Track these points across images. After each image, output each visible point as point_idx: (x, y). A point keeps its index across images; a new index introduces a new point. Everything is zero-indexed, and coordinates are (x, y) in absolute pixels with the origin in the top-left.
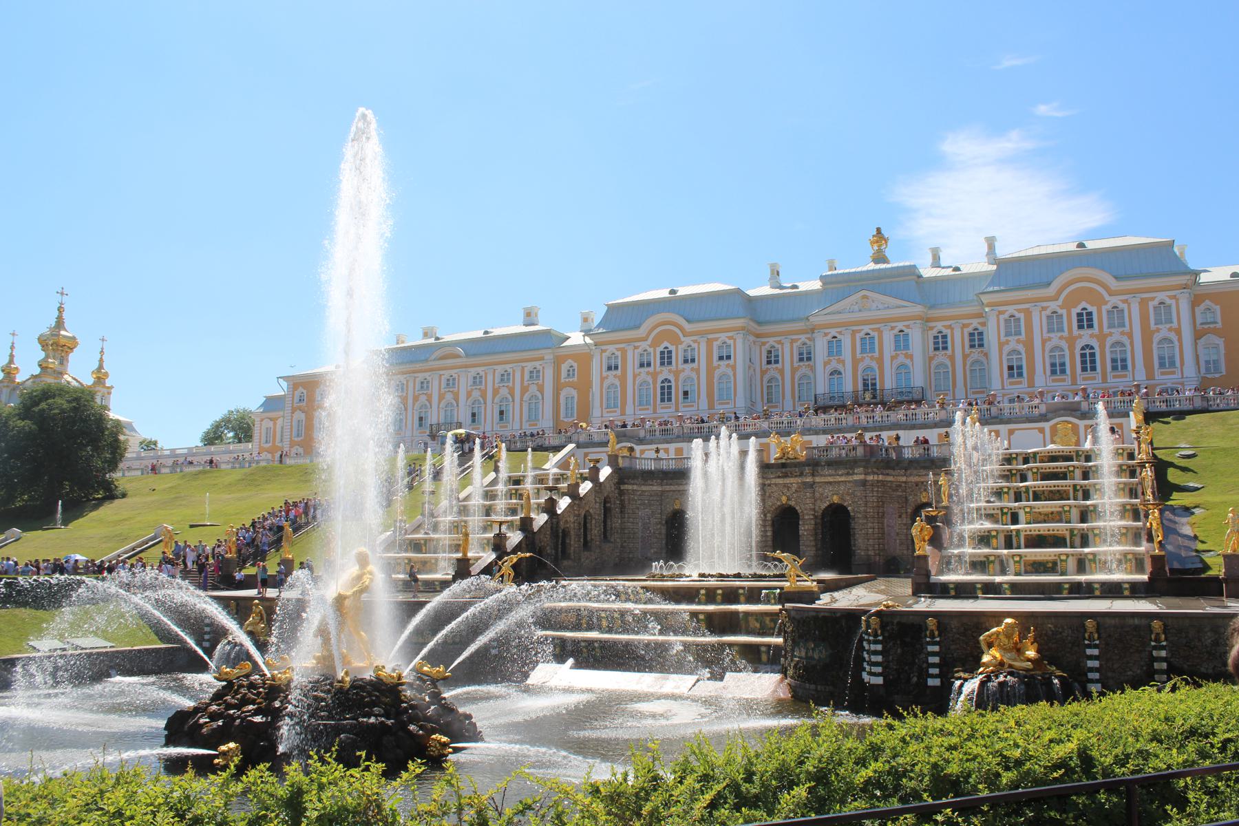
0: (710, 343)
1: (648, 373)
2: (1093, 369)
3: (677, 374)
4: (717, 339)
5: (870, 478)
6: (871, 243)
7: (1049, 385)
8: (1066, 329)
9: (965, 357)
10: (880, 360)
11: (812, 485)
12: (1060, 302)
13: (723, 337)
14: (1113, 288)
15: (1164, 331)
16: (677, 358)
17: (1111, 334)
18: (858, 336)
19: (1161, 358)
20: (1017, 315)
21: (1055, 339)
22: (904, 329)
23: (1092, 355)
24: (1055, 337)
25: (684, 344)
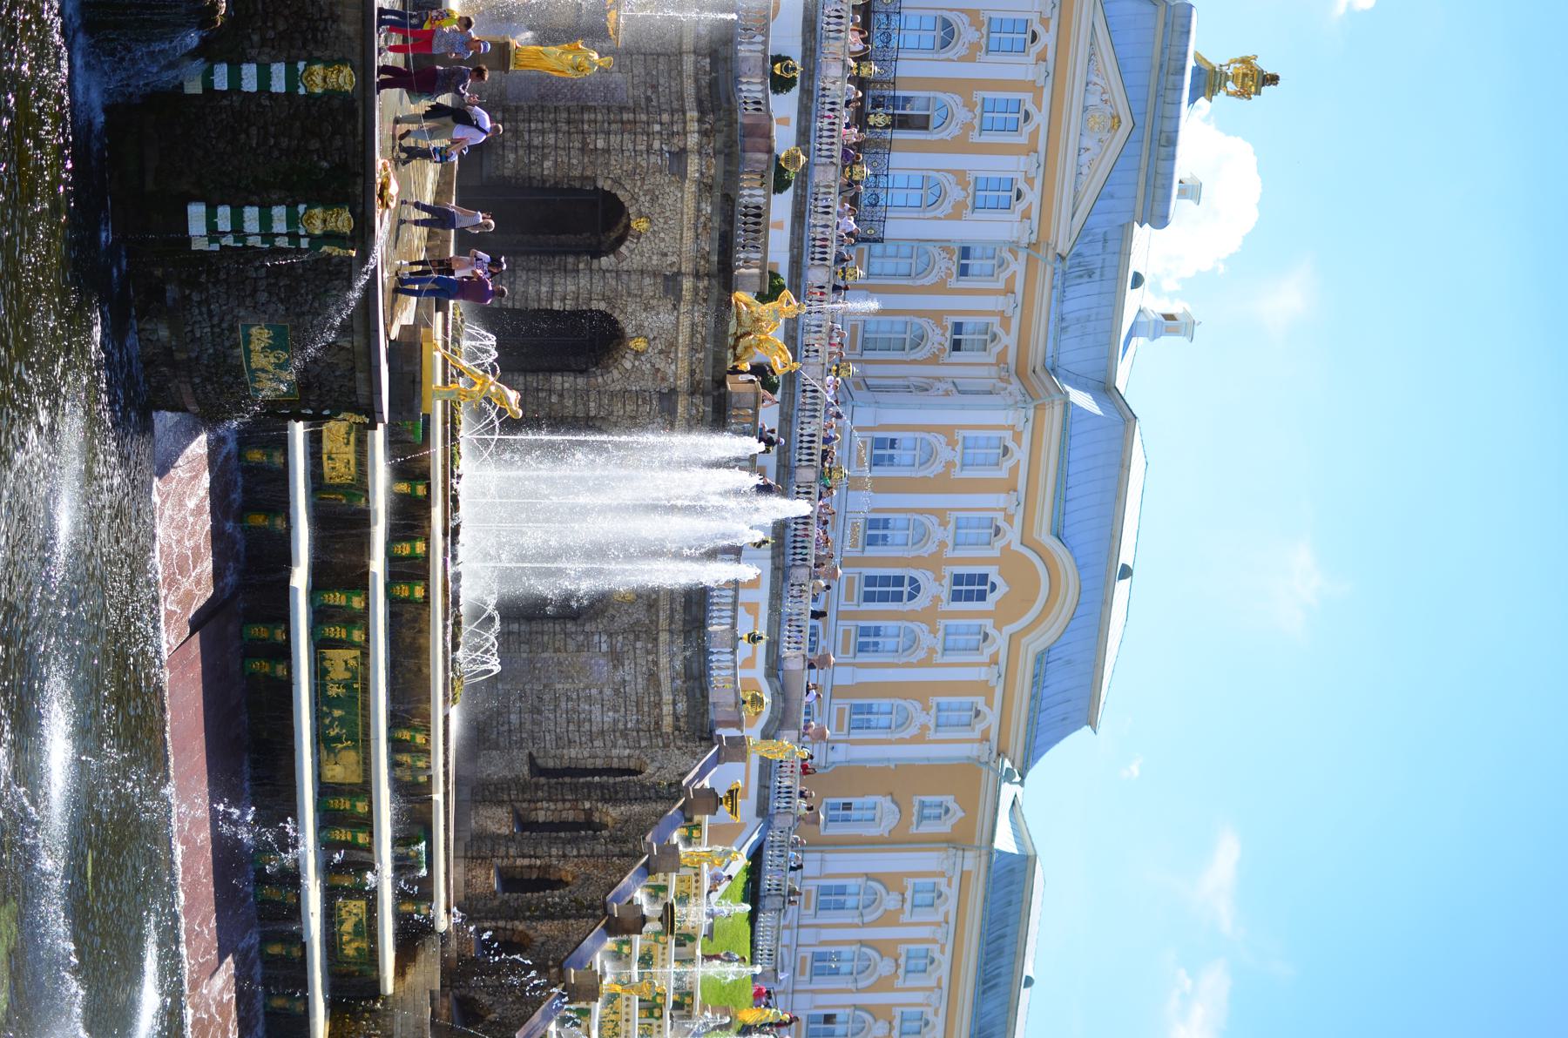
2: (869, 597)
6: (1244, 61)
7: (848, 515)
8: (961, 553)
9: (937, 316)
10: (961, 146)
12: (1016, 546)
14: (1024, 641)
15: (920, 718)
17: (933, 631)
18: (1027, 97)
20: (1007, 464)
21: (938, 533)
22: (1021, 206)
23: (898, 597)
24: (948, 534)
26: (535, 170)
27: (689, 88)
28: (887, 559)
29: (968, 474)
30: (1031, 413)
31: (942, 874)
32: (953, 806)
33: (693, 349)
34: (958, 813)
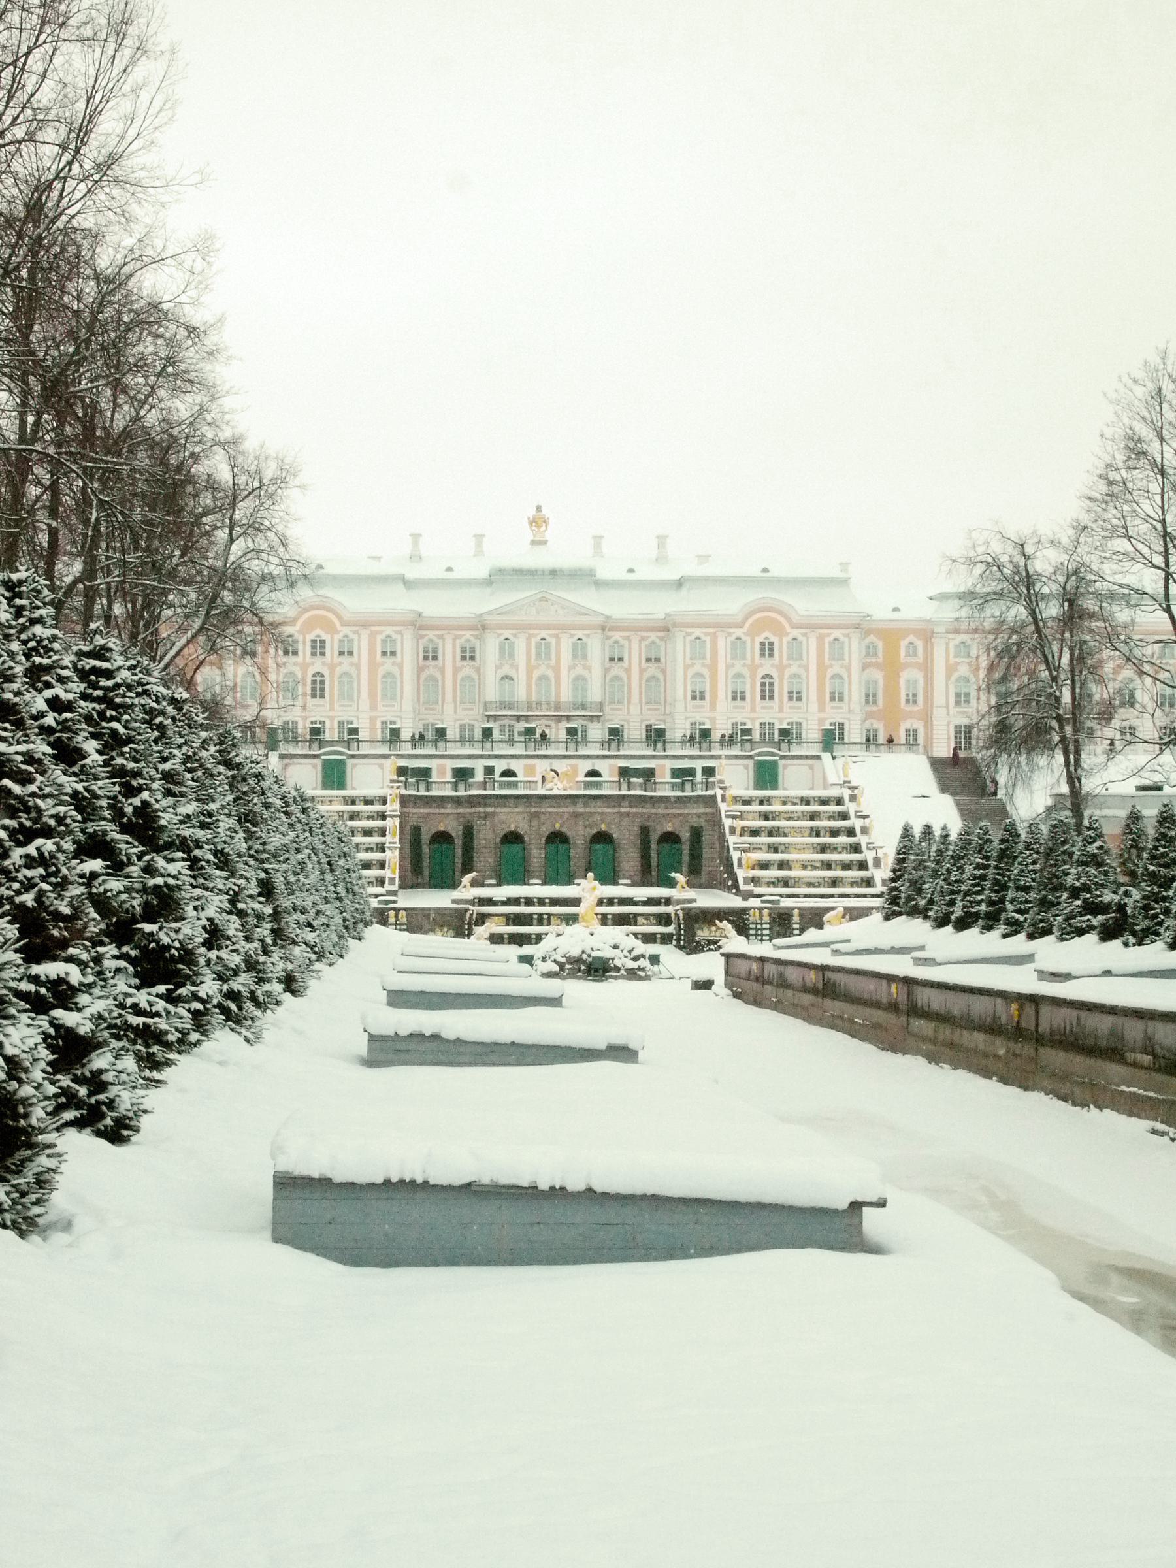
0: (372, 636)
1: (295, 664)
2: (771, 698)
3: (332, 667)
4: (381, 632)
5: (634, 810)
6: (531, 523)
8: (748, 656)
9: (642, 671)
10: (557, 669)
11: (582, 814)
13: (389, 630)
15: (836, 669)
16: (332, 649)
17: (789, 666)
18: (534, 641)
19: (832, 694)
20: (703, 638)
21: (738, 667)
22: (584, 639)
25: (340, 636)
26: (492, 864)
27: (469, 810)
28: (753, 691)
29: (708, 656)
30: (677, 629)
31: (947, 644)
32: (906, 641)
33: (559, 807)
34: (911, 638)
